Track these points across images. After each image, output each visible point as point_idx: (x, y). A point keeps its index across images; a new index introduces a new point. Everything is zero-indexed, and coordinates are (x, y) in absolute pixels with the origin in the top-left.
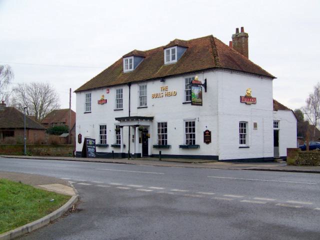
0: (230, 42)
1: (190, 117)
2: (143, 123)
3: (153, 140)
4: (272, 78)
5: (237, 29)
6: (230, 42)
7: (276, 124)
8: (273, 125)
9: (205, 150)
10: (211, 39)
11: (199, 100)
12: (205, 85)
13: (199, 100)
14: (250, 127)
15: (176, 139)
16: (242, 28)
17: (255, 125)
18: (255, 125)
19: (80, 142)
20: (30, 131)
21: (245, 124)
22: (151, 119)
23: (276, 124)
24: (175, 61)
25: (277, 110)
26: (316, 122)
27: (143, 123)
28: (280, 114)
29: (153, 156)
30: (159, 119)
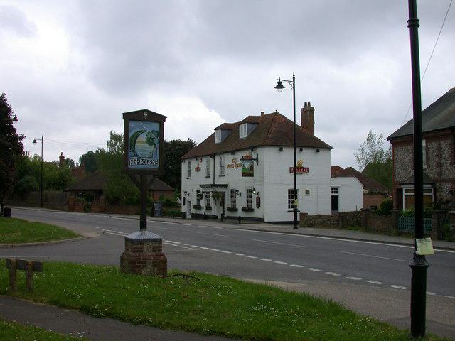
0: (160, 119)
1: (249, 185)
2: (219, 190)
3: (228, 203)
4: (330, 148)
5: (306, 103)
6: (160, 119)
7: (335, 190)
8: (331, 191)
9: (257, 213)
10: (277, 114)
11: (251, 172)
12: (257, 160)
13: (251, 172)
14: (301, 194)
15: (241, 202)
16: (309, 102)
17: (307, 192)
18: (307, 192)
19: (184, 204)
20: (155, 193)
21: (337, 189)
22: (226, 186)
23: (335, 190)
24: (246, 136)
25: (335, 178)
26: (378, 193)
27: (219, 190)
28: (340, 182)
29: (228, 217)
30: (232, 186)
